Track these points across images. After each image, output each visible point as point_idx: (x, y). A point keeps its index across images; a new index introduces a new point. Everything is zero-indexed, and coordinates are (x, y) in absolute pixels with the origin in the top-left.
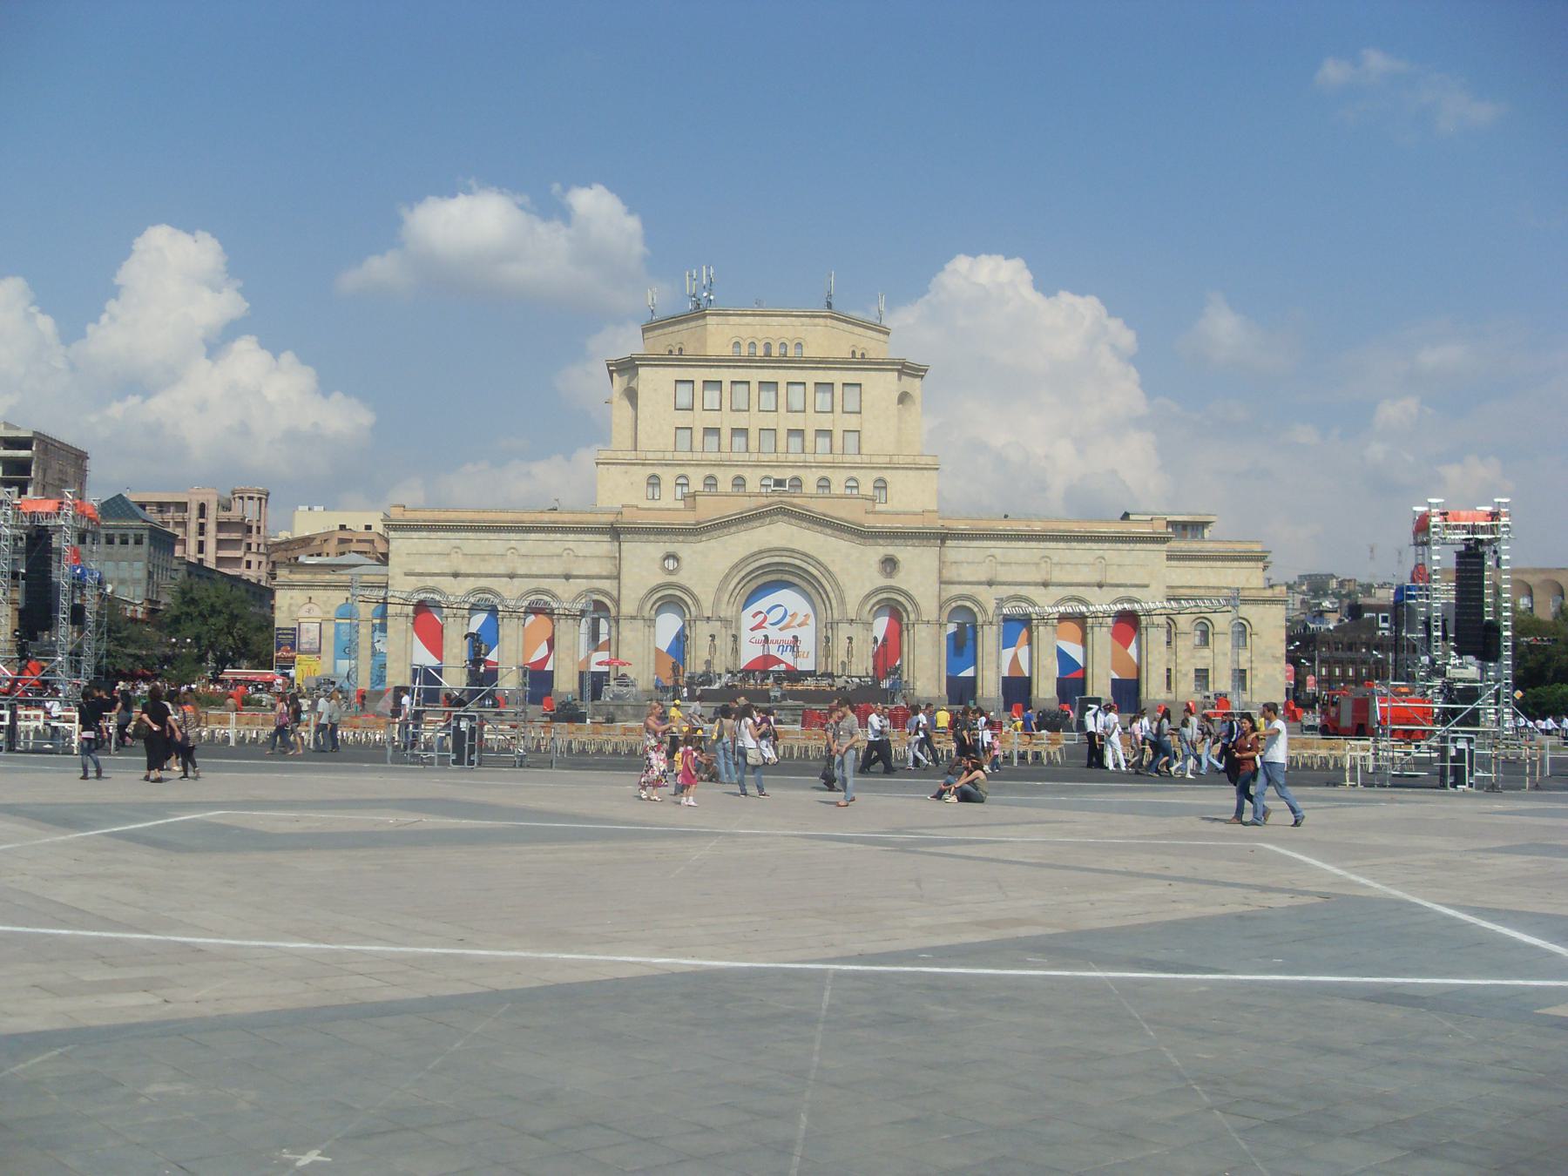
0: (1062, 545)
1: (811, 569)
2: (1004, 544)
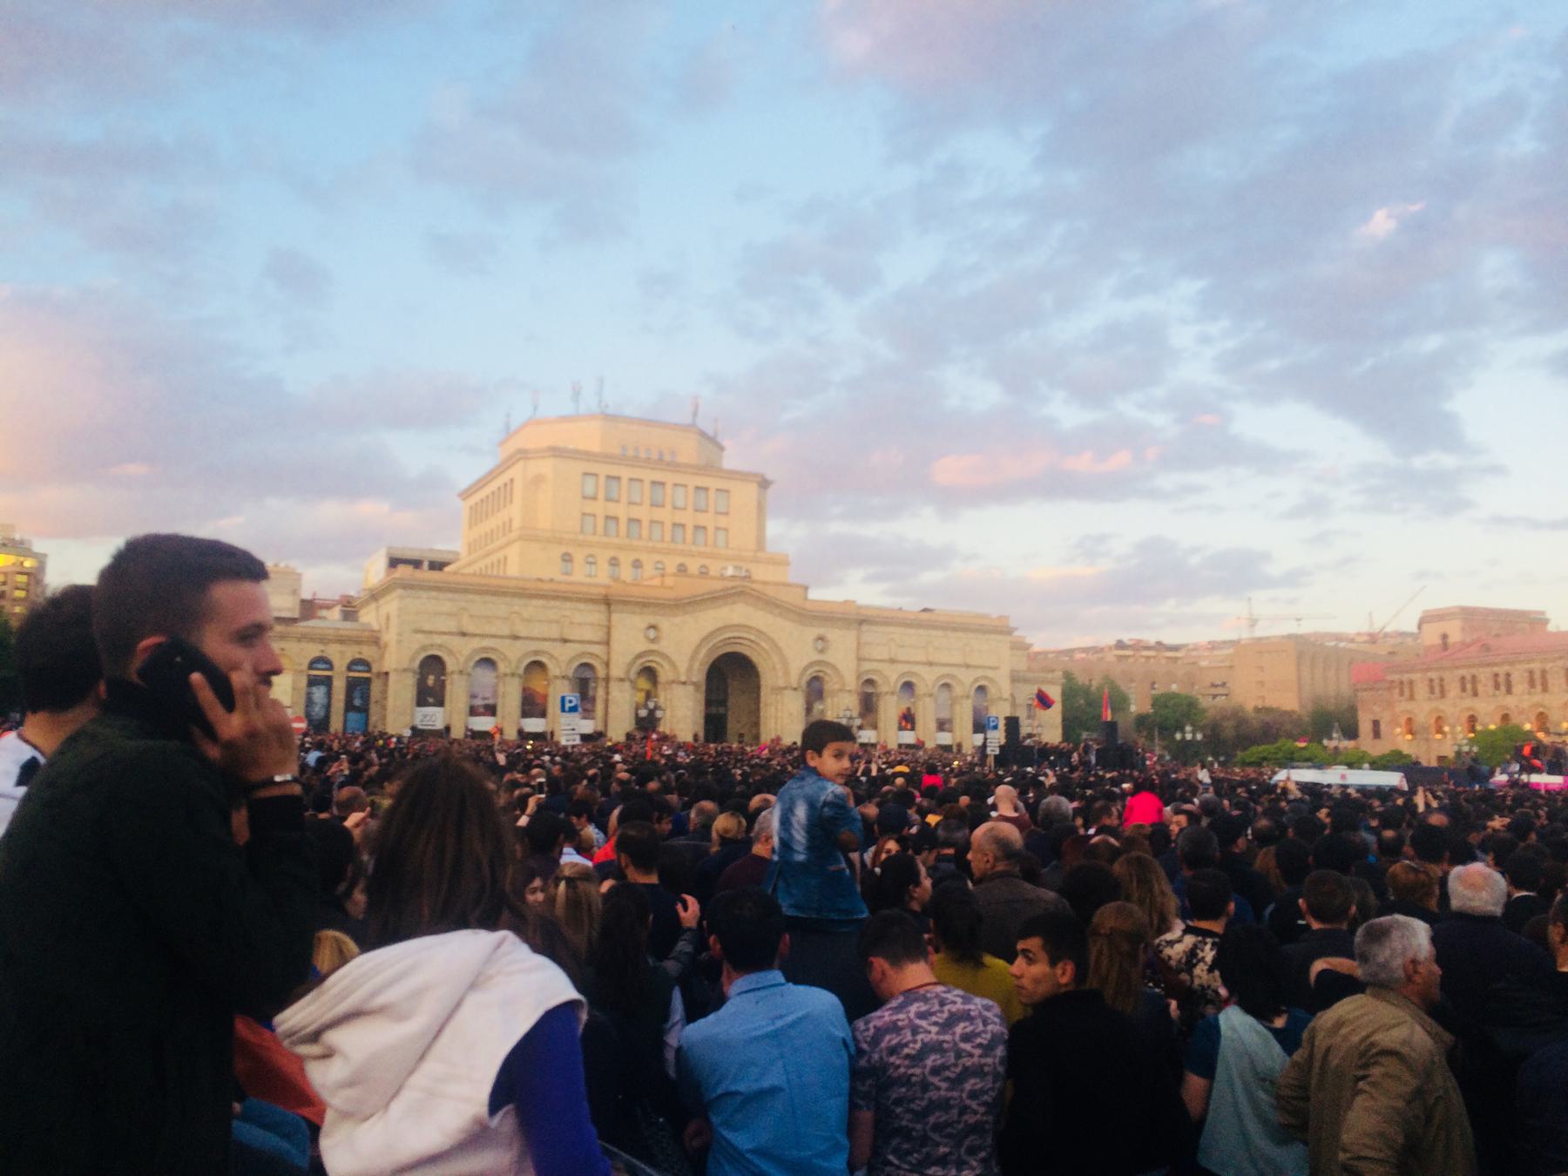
0: (940, 633)
2: (901, 630)
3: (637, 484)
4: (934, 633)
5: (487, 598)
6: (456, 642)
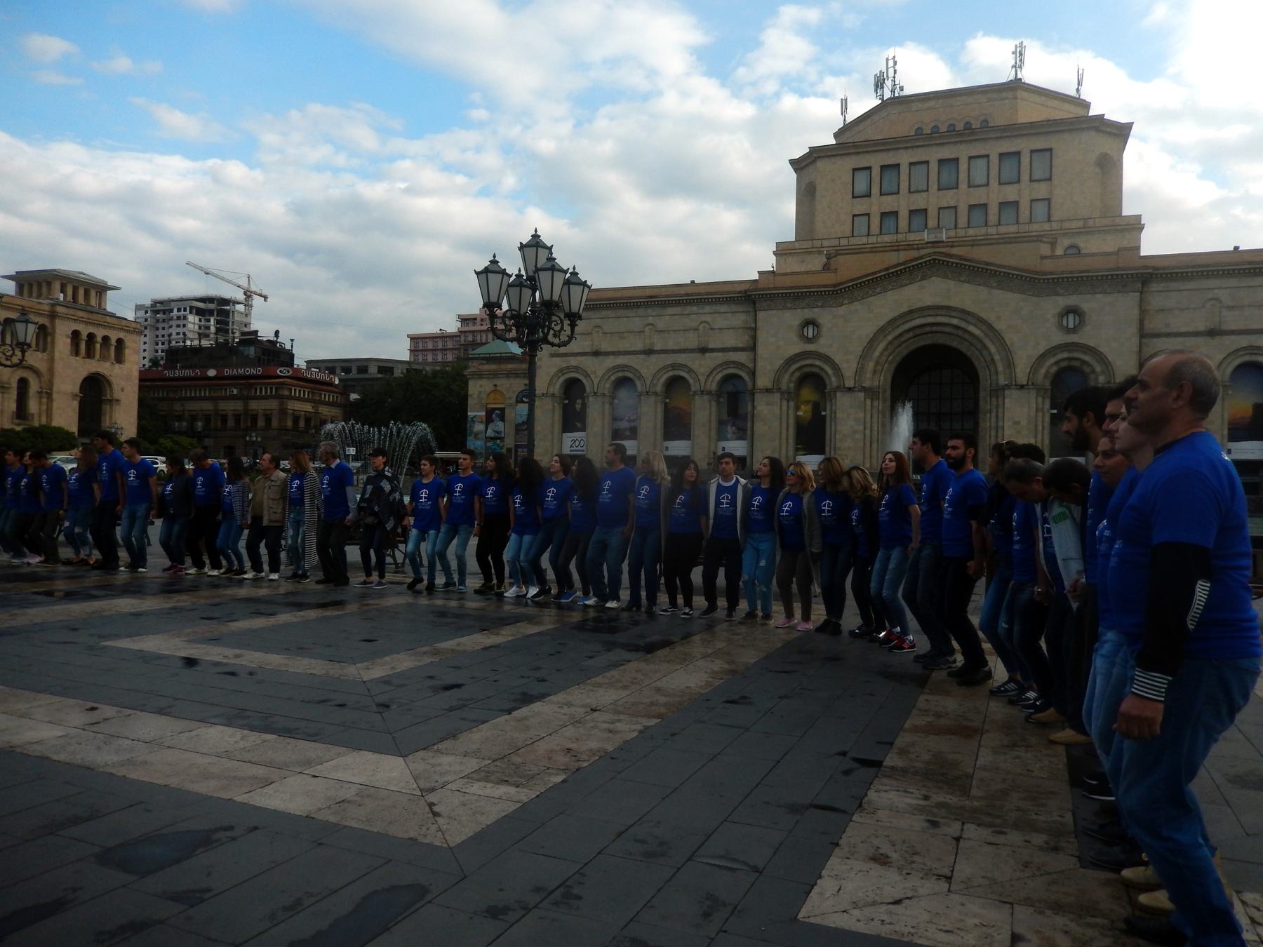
1: (971, 328)
2: (1232, 282)
5: (621, 312)
6: (589, 363)
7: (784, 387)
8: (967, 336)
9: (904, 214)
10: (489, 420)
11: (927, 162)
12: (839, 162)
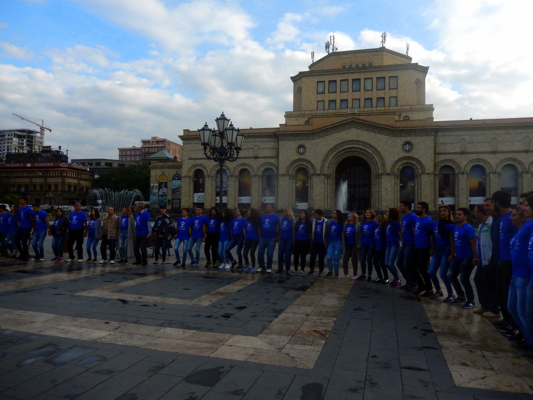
0: (503, 132)
1: (368, 150)
2: (470, 133)
3: (346, 82)
4: (498, 132)
7: (290, 173)
8: (366, 153)
9: (338, 102)
10: (160, 187)
11: (348, 80)
12: (311, 78)
